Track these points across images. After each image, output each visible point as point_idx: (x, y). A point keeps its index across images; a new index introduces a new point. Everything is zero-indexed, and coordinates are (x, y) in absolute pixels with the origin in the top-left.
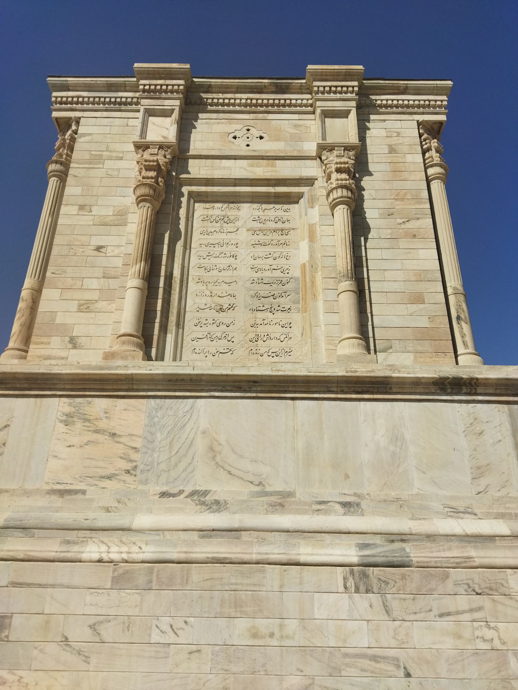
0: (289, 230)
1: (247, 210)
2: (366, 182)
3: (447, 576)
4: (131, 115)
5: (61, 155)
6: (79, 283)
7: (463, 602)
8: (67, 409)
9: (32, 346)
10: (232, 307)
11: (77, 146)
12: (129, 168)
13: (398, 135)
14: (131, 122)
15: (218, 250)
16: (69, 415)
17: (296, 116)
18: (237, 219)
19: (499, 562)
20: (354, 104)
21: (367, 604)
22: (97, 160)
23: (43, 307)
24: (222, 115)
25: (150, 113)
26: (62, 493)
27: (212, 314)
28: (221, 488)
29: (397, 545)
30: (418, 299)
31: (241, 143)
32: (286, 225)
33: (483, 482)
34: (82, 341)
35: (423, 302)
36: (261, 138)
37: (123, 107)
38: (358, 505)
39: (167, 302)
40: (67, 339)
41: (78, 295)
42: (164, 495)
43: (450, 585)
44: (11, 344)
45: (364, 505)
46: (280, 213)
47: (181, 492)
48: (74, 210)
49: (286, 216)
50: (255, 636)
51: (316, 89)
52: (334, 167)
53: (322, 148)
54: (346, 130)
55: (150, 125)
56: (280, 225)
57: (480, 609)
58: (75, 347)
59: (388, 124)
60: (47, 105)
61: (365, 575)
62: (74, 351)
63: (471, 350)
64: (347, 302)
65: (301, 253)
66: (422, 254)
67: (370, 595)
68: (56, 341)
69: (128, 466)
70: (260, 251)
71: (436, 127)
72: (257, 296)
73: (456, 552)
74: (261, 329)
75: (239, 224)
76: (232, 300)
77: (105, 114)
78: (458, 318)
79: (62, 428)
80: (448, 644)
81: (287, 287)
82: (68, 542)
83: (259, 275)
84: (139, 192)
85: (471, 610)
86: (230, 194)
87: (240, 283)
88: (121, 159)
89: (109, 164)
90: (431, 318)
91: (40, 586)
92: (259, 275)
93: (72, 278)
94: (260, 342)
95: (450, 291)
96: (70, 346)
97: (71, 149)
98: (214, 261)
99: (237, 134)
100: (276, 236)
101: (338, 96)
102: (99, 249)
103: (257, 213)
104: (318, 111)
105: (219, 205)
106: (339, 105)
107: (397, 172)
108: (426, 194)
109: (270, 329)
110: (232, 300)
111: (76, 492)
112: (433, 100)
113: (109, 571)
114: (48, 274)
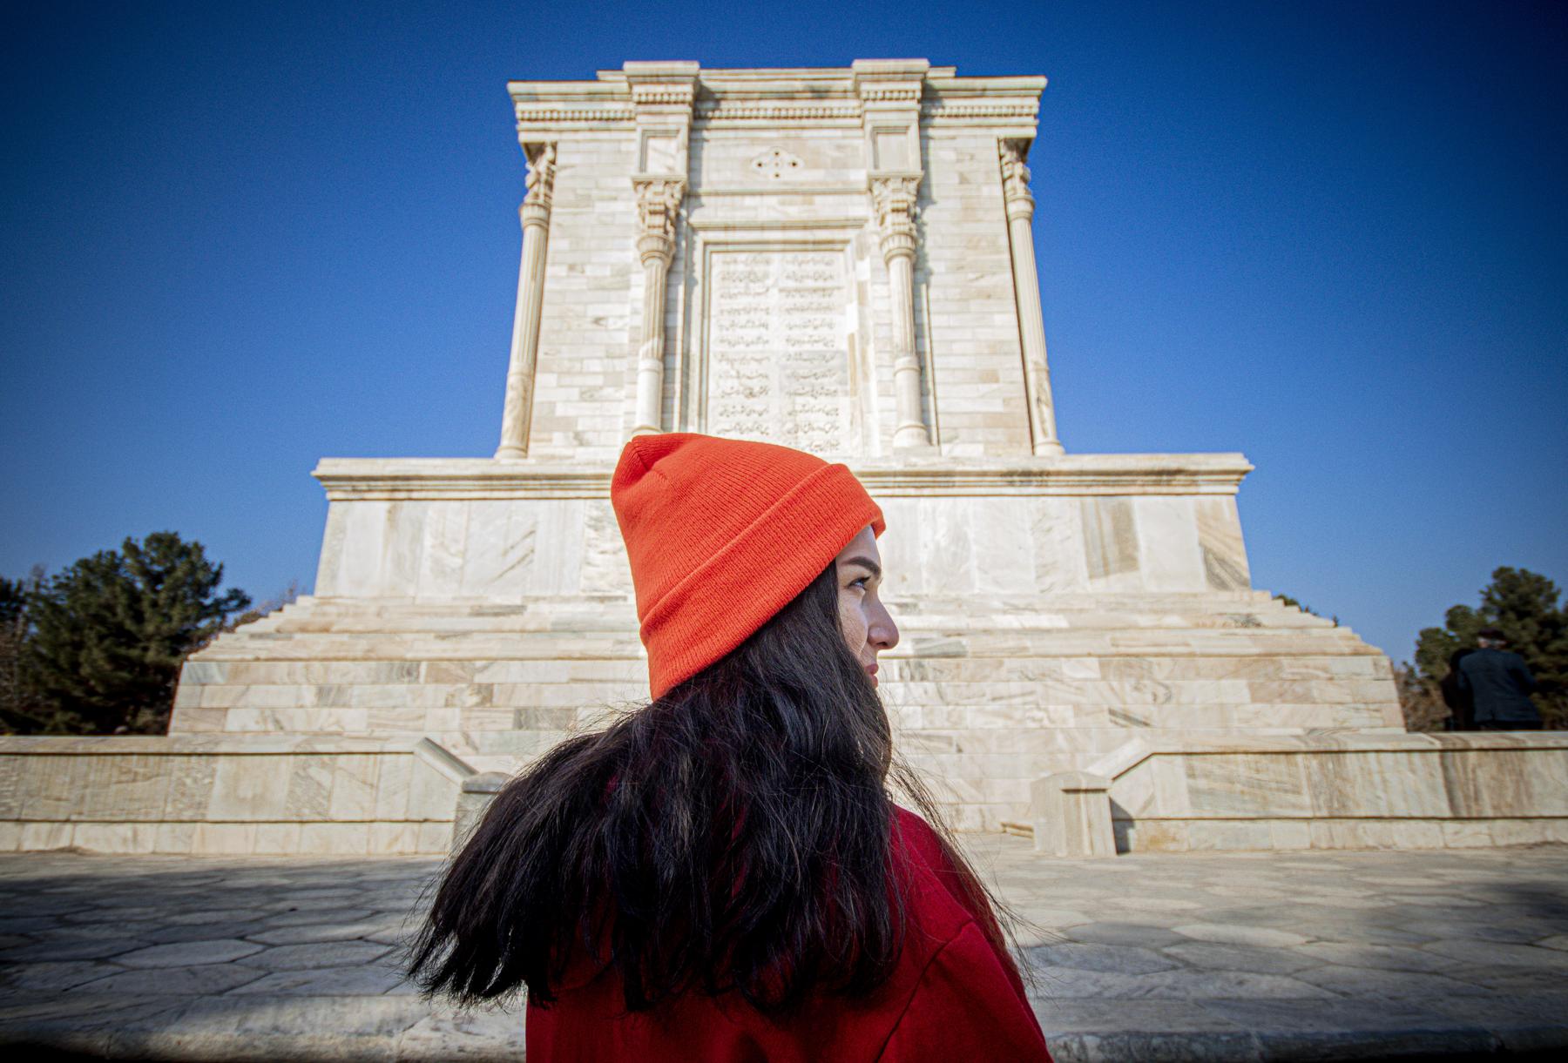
0: (833, 289)
1: (778, 265)
2: (929, 215)
3: (1001, 664)
4: (624, 135)
5: (537, 196)
6: (578, 366)
7: (1015, 687)
8: (595, 513)
9: (532, 445)
10: (764, 391)
11: (557, 183)
12: (627, 209)
13: (972, 157)
14: (624, 147)
15: (743, 318)
16: (597, 520)
17: (839, 133)
18: (766, 276)
19: (1054, 651)
20: (915, 116)
21: (921, 691)
23: (539, 397)
24: (741, 134)
25: (648, 135)
26: (602, 599)
27: (739, 400)
29: (953, 639)
30: (991, 377)
31: (768, 171)
32: (829, 284)
33: (1048, 580)
34: (589, 436)
35: (997, 381)
37: (612, 125)
38: (915, 606)
39: (685, 387)
40: (571, 435)
41: (578, 380)
43: (1003, 672)
44: (505, 442)
45: (921, 605)
46: (821, 268)
48: (562, 271)
49: (828, 270)
51: (864, 95)
52: (888, 207)
53: (872, 180)
54: (902, 153)
55: (651, 153)
56: (820, 284)
57: (1031, 693)
58: (581, 444)
59: (958, 143)
60: (511, 122)
61: (920, 666)
62: (581, 450)
63: (1052, 437)
64: (905, 381)
65: (848, 321)
66: (999, 319)
67: (926, 684)
68: (558, 437)
70: (797, 318)
71: (1022, 145)
72: (794, 376)
73: (1011, 643)
74: (801, 418)
75: (769, 282)
76: (764, 382)
77: (589, 135)
78: (1038, 400)
79: (591, 533)
81: (833, 363)
82: (621, 642)
83: (797, 348)
84: (646, 246)
85: (1023, 695)
86: (756, 240)
87: (773, 360)
88: (615, 199)
89: (600, 207)
90: (1006, 402)
91: (601, 681)
92: (797, 348)
93: (570, 360)
94: (800, 434)
95: (1030, 366)
97: (550, 185)
98: (740, 332)
99: (763, 160)
100: (816, 299)
101: (894, 105)
102: (597, 321)
103: (791, 268)
104: (868, 128)
105: (742, 257)
106: (893, 119)
107: (969, 210)
108: (1004, 241)
109: (812, 417)
110: (764, 382)
111: (617, 598)
112: (1016, 102)
114: (540, 355)
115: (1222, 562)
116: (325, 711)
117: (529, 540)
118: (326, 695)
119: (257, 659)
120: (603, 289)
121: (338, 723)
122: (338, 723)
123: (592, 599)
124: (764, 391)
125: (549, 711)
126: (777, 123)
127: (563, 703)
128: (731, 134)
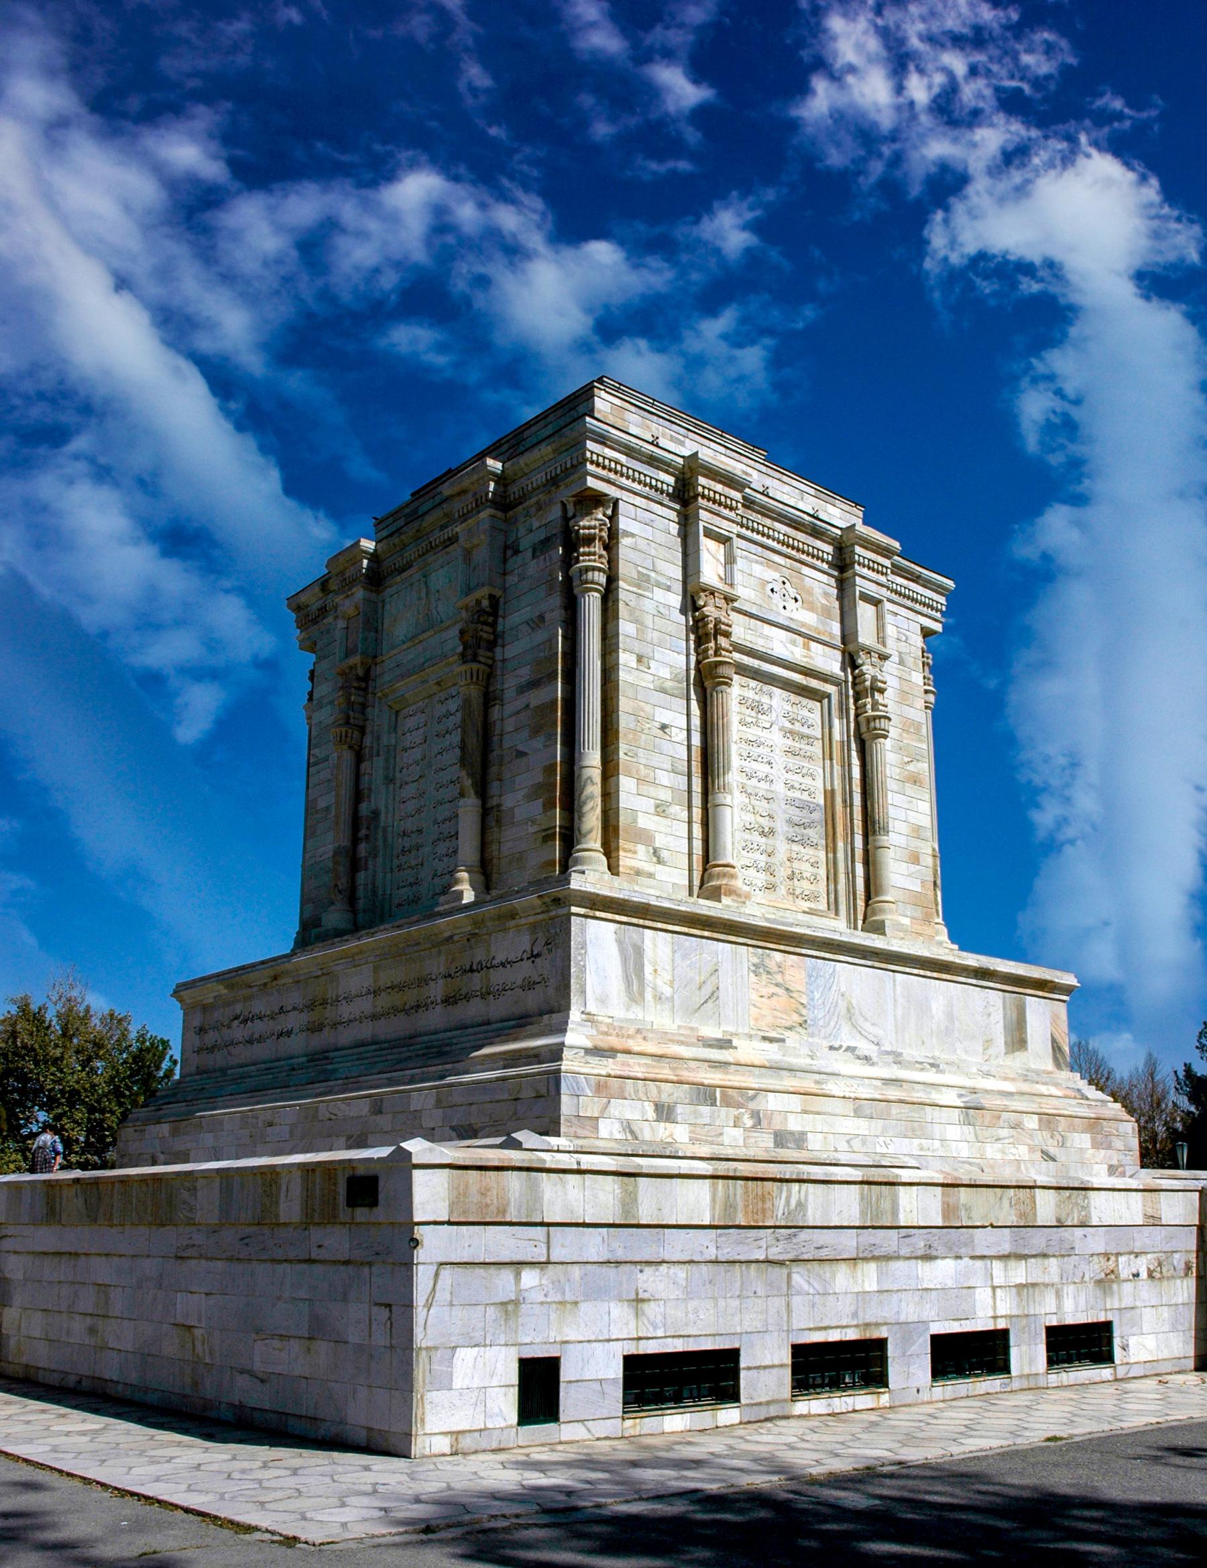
19: (1020, 1109)
22: (643, 581)
28: (865, 1047)
34: (664, 854)
36: (796, 600)
41: (652, 791)
42: (831, 1048)
47: (841, 1047)
50: (921, 1149)
56: (805, 730)
58: (659, 862)
68: (641, 849)
69: (800, 1020)
70: (793, 762)
80: (999, 1156)
83: (790, 794)
96: (655, 859)
98: (755, 765)
102: (664, 727)
113: (850, 1105)
115: (1060, 1049)
116: (662, 1124)
117: (714, 977)
118: (665, 1112)
119: (609, 1076)
120: (663, 691)
121: (671, 1136)
122: (671, 1136)
123: (764, 1038)
124: (772, 831)
125: (792, 1133)
126: (784, 549)
127: (799, 1129)
128: (753, 547)
